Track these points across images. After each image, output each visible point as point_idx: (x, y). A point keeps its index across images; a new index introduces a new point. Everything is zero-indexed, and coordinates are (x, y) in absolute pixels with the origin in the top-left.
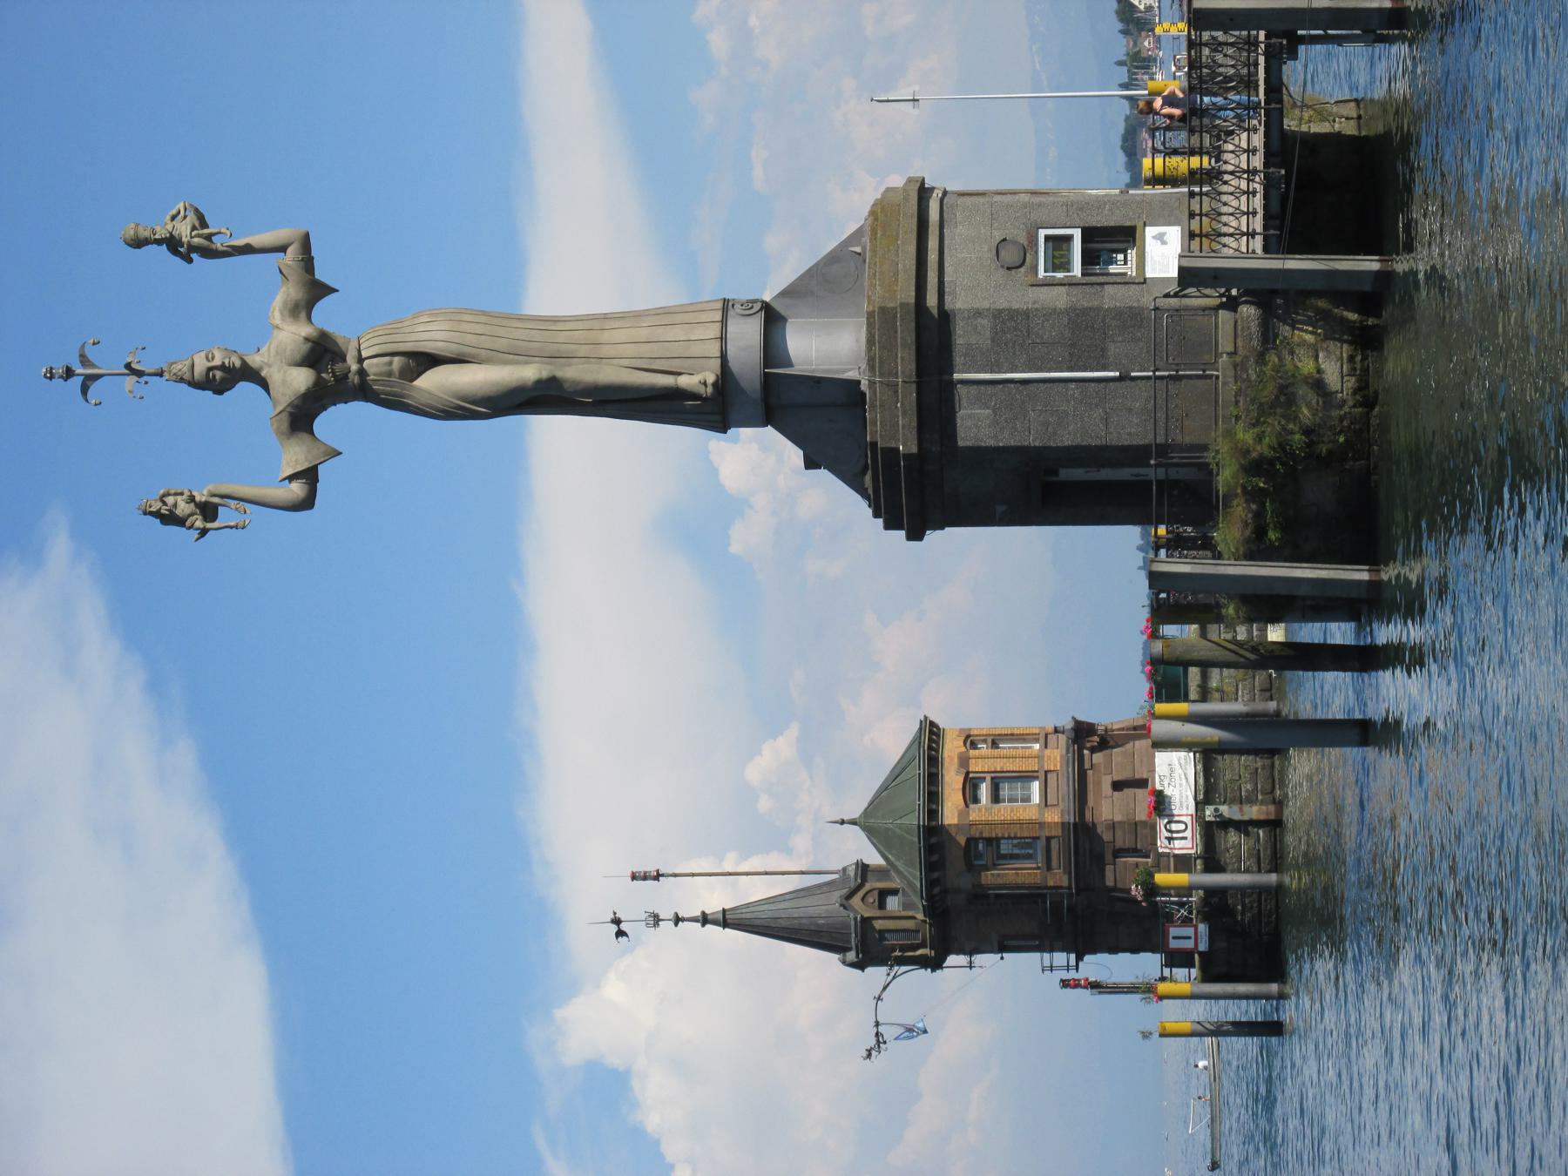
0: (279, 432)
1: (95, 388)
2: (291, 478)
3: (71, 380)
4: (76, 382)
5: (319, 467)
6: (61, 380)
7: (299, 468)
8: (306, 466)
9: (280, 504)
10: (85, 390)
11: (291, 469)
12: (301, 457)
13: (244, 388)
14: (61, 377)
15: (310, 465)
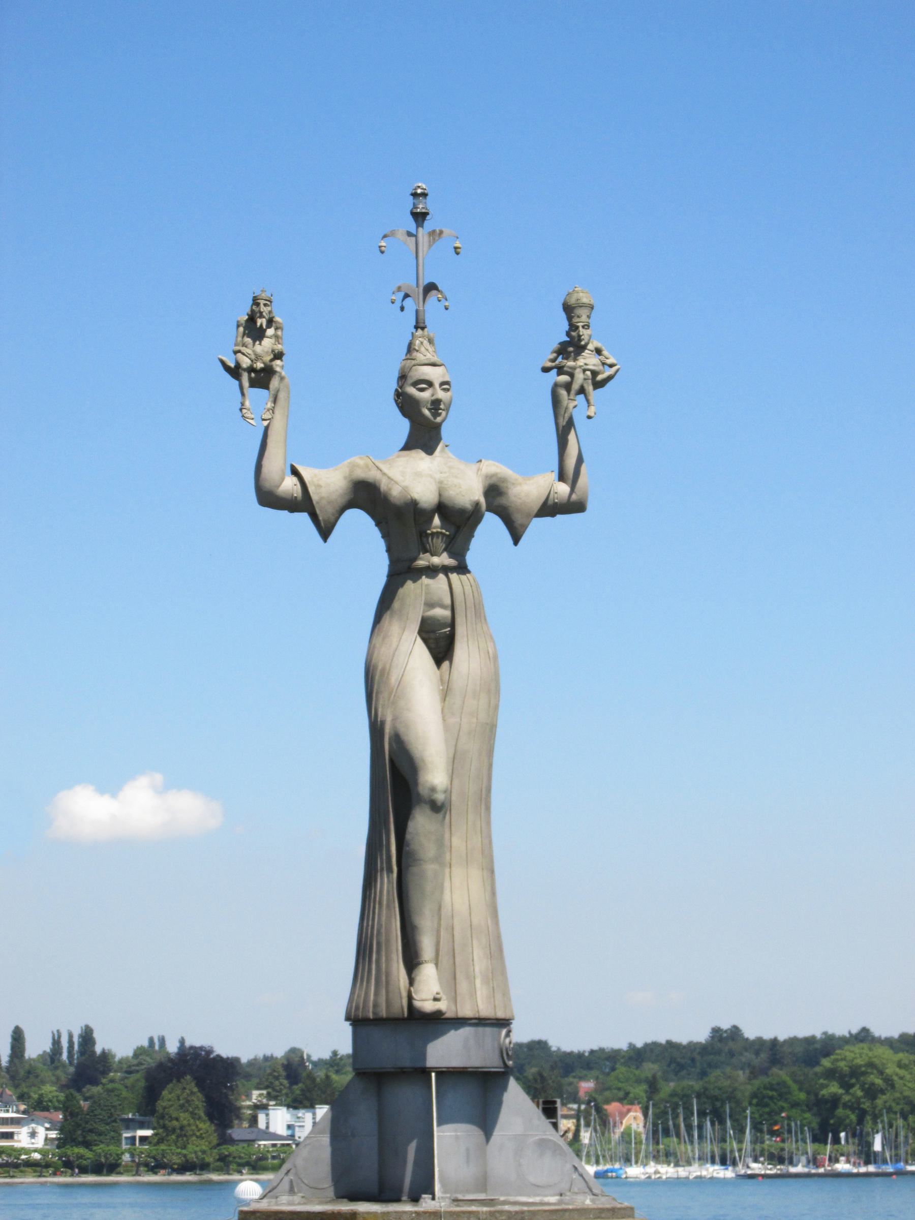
3: (411, 219)
6: (410, 207)
7: (311, 489)
11: (310, 479)
12: (324, 492)
14: (415, 207)
15: (314, 503)
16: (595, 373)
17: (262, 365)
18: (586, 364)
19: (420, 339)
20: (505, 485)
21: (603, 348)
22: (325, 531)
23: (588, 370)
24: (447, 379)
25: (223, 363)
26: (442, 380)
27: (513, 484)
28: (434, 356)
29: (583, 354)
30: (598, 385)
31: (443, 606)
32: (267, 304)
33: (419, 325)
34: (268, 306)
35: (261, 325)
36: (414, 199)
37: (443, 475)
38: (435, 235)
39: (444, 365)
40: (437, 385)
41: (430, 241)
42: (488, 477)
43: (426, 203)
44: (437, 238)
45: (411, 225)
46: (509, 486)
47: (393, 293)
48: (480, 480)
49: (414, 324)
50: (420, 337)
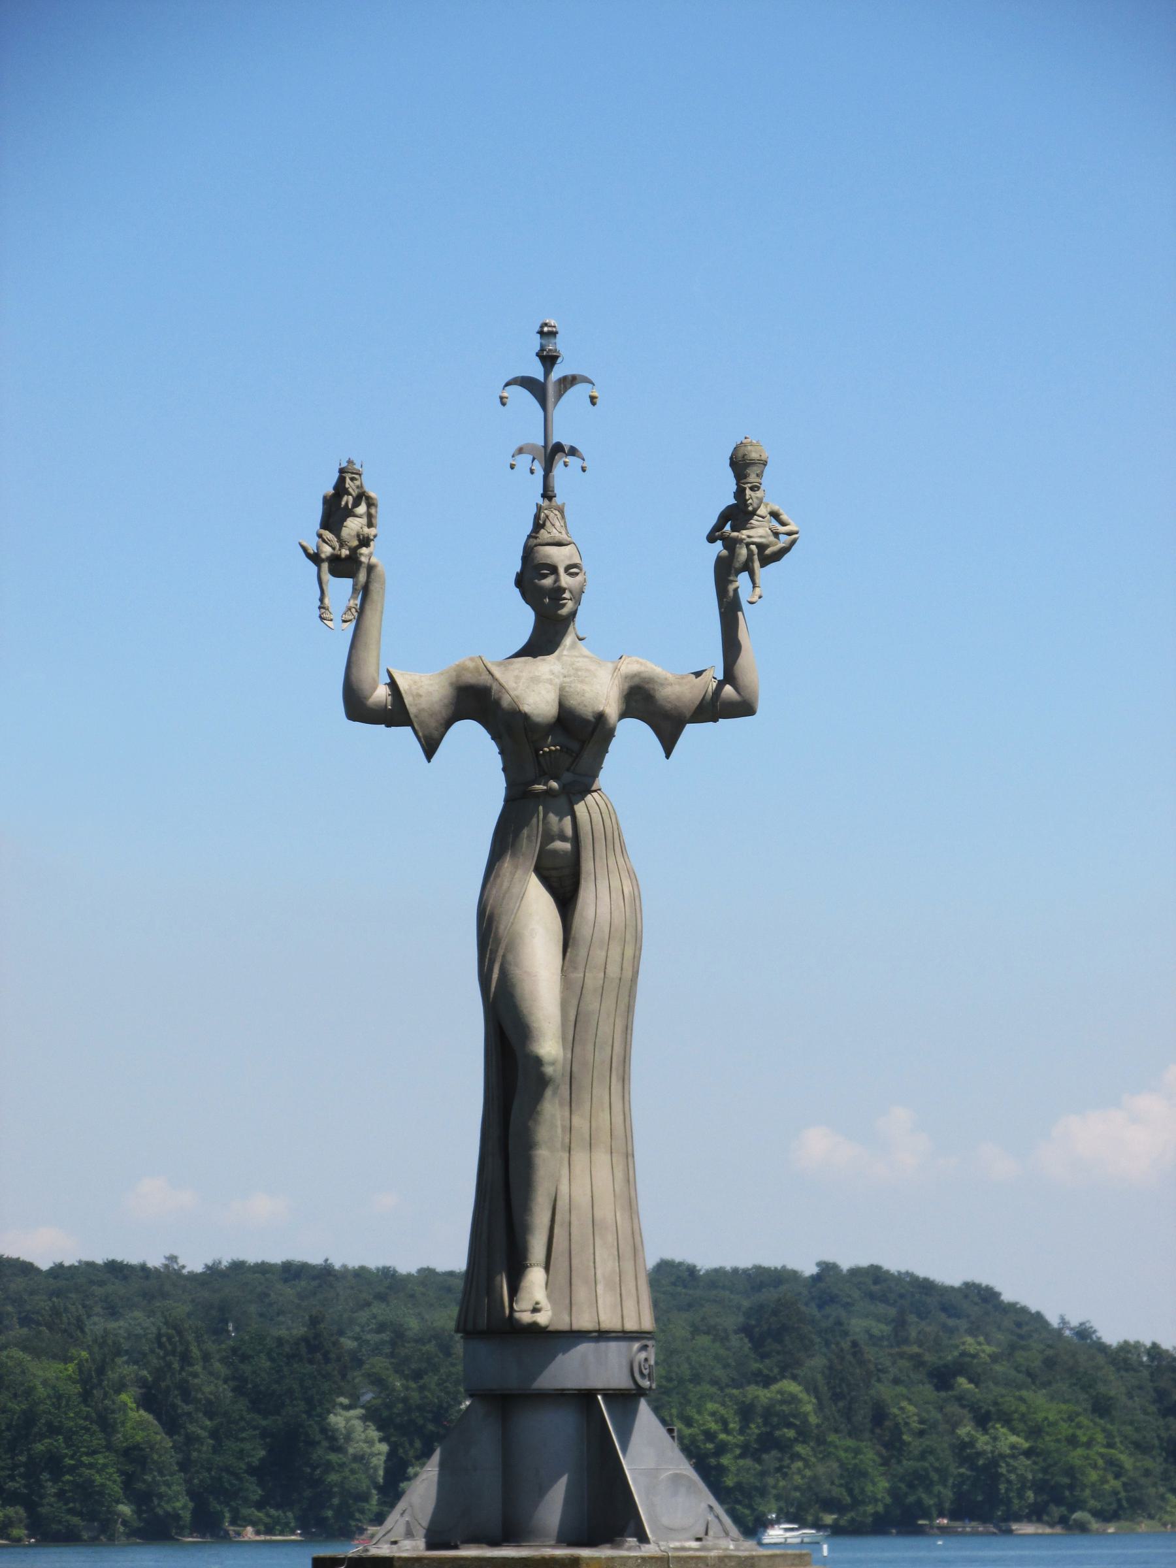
0: (461, 669)
1: (523, 398)
2: (393, 685)
4: (536, 371)
5: (409, 728)
6: (538, 348)
7: (408, 700)
8: (412, 710)
9: (354, 670)
10: (526, 383)
11: (407, 687)
12: (424, 703)
13: (522, 621)
14: (542, 349)
15: (412, 716)
16: (762, 547)
17: (348, 552)
18: (749, 537)
19: (546, 511)
20: (651, 686)
21: (781, 511)
22: (430, 748)
23: (753, 543)
24: (577, 560)
25: (305, 549)
26: (568, 562)
27: (662, 685)
28: (560, 533)
29: (752, 521)
30: (766, 560)
31: (563, 838)
32: (354, 477)
33: (548, 494)
34: (356, 479)
35: (347, 503)
36: (541, 338)
37: (567, 680)
38: (568, 382)
39: (574, 544)
40: (561, 570)
41: (560, 390)
42: (628, 677)
43: (555, 343)
44: (568, 386)
45: (536, 371)
46: (656, 687)
47: (513, 456)
48: (616, 682)
49: (542, 492)
50: (546, 509)
